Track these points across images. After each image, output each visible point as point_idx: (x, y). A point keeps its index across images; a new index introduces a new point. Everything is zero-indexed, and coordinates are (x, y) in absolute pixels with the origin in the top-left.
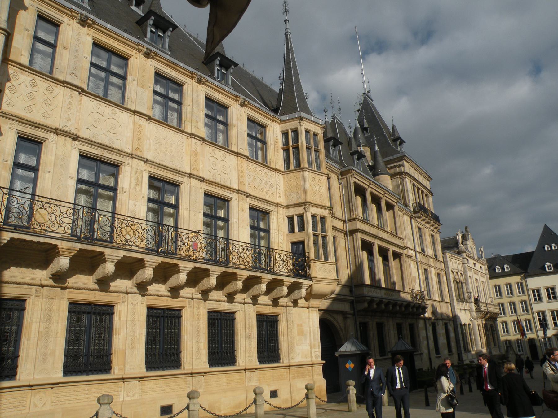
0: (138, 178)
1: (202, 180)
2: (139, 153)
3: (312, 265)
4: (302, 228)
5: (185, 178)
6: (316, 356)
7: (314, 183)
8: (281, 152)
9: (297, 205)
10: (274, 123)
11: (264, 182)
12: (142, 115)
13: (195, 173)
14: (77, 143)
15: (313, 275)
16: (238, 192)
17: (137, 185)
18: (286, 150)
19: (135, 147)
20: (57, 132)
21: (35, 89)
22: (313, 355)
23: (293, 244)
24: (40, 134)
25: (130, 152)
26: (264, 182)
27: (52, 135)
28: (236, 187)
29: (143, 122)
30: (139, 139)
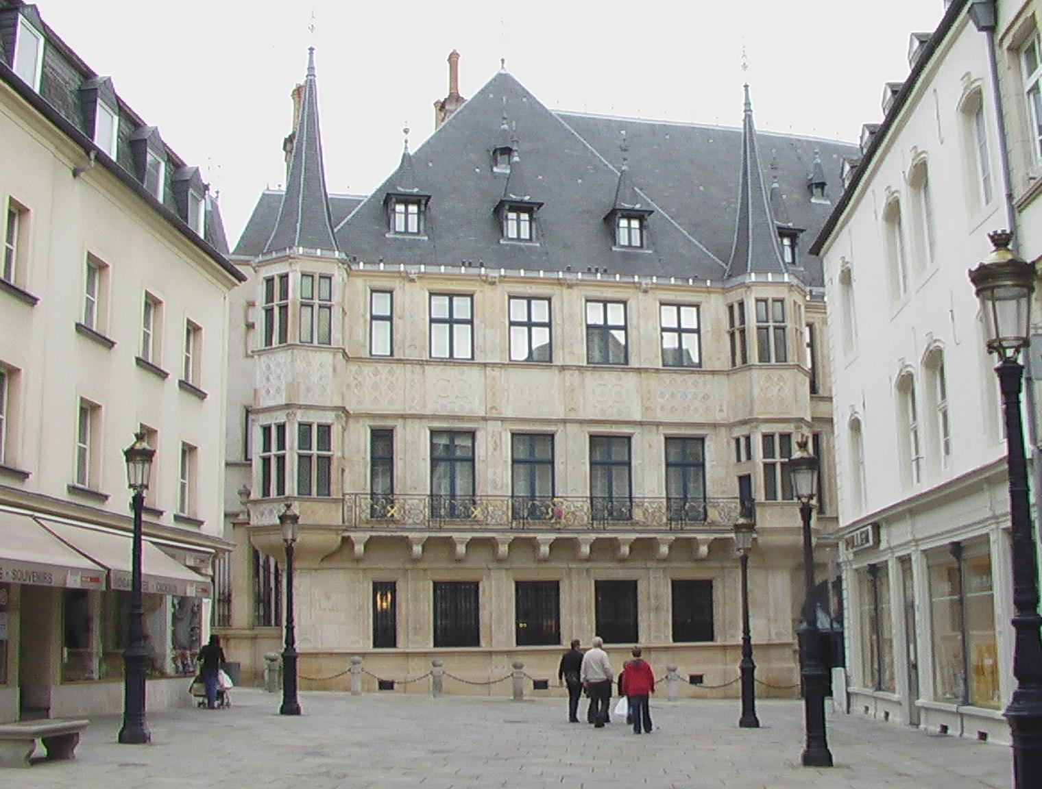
0: (495, 442)
1: (582, 422)
2: (494, 414)
3: (758, 511)
4: (749, 457)
5: (559, 424)
6: (778, 634)
7: (769, 384)
8: (727, 338)
9: (744, 422)
10: (712, 295)
11: (690, 396)
12: (494, 365)
13: (573, 416)
14: (424, 421)
15: (759, 525)
16: (641, 423)
17: (495, 449)
18: (732, 335)
19: (489, 406)
20: (403, 417)
21: (379, 376)
22: (773, 635)
23: (741, 478)
24: (388, 423)
25: (483, 414)
26: (690, 396)
27: (400, 420)
28: (638, 417)
29: (496, 372)
30: (494, 394)
